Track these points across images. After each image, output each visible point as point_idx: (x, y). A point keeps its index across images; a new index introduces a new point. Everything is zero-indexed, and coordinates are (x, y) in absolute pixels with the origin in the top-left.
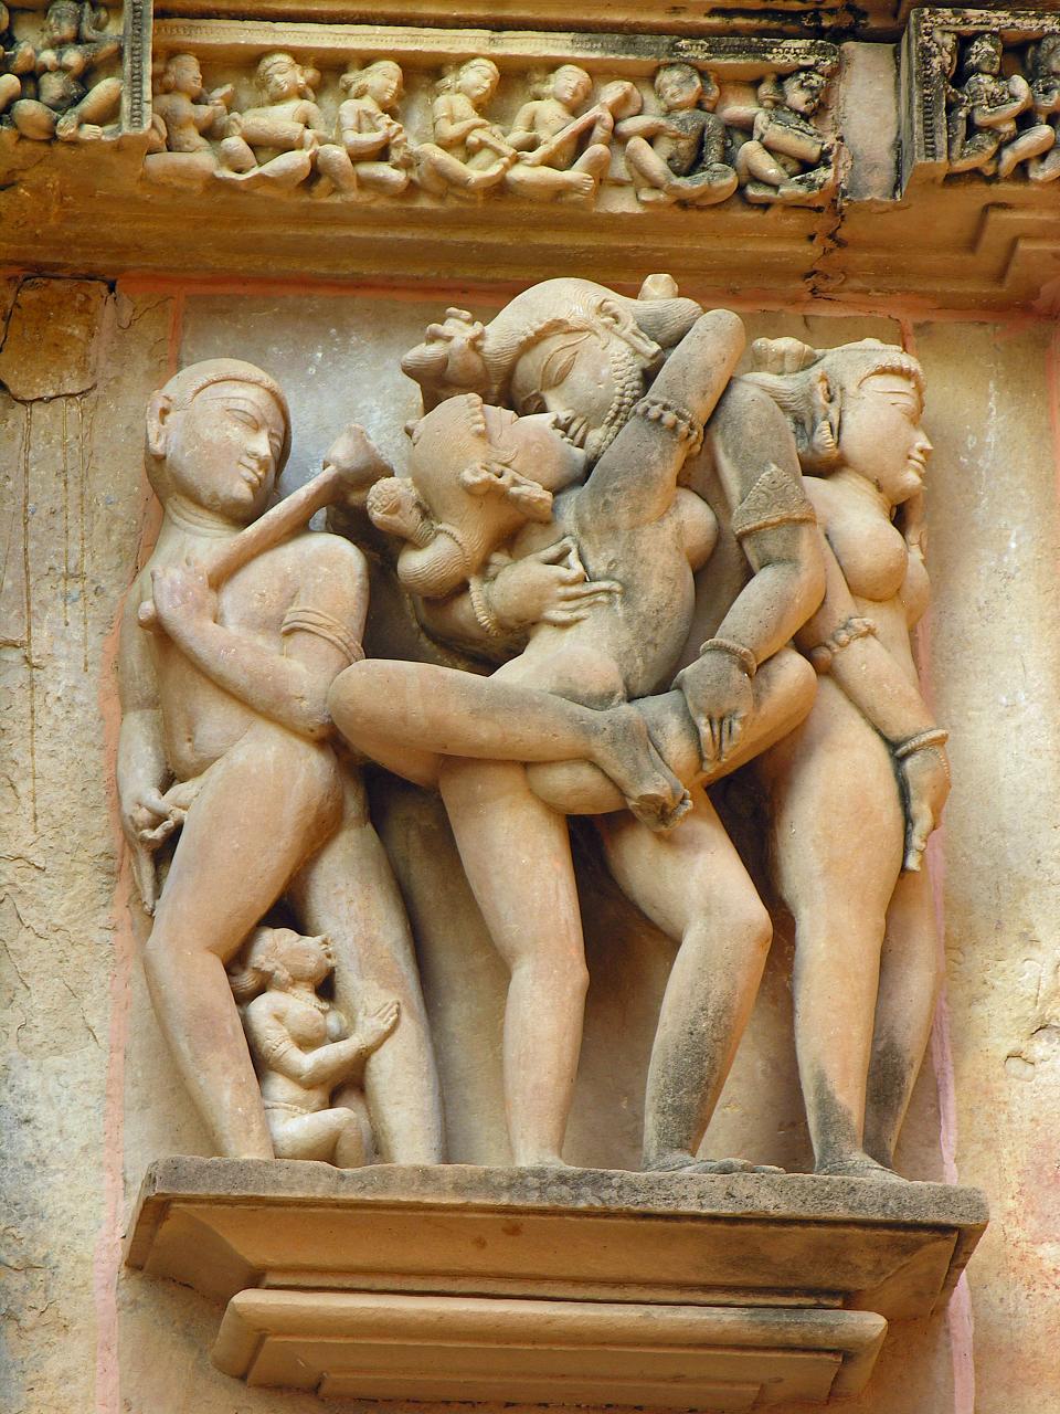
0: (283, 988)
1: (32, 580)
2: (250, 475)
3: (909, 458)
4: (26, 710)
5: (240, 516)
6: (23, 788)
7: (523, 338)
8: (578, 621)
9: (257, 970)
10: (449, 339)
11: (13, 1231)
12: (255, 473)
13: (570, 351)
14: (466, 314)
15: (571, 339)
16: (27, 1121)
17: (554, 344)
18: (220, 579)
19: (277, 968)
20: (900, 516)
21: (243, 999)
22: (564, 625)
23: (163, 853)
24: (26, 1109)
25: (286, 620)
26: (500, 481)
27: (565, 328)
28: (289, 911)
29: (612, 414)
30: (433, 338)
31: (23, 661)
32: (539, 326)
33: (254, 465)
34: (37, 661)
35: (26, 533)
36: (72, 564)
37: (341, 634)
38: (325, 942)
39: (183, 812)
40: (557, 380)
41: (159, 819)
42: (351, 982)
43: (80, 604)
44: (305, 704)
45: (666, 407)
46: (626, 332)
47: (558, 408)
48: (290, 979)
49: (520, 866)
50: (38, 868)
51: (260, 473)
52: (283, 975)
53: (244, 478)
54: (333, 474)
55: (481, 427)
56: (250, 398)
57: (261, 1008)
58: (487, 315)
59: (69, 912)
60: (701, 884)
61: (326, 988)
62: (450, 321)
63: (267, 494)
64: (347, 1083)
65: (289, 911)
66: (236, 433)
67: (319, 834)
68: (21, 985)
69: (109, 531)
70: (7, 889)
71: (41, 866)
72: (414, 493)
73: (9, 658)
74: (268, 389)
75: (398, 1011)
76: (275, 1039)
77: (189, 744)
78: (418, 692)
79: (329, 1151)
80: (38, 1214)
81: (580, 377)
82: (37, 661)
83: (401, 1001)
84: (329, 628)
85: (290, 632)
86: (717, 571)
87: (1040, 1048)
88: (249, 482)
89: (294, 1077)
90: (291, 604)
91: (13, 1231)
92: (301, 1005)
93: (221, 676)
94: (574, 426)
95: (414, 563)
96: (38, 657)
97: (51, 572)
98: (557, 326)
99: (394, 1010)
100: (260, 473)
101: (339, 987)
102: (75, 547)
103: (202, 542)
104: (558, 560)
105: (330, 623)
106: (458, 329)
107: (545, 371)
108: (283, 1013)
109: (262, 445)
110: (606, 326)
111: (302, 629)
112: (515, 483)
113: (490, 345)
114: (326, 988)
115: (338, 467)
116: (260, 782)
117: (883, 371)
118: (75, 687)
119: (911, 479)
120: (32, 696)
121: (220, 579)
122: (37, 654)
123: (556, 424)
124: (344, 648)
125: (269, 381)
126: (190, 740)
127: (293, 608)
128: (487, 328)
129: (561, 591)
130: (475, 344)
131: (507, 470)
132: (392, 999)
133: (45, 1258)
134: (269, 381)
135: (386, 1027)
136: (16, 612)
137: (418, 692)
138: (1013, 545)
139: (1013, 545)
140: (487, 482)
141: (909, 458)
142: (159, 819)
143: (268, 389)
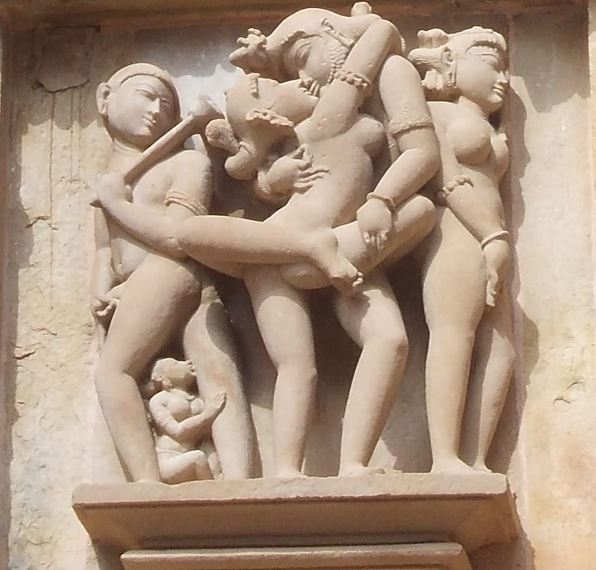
0: (168, 389)
1: (53, 184)
2: (150, 123)
3: (494, 88)
4: (48, 251)
5: (142, 143)
6: (47, 292)
7: (283, 42)
8: (309, 187)
9: (154, 381)
10: (247, 46)
11: (34, 524)
12: (151, 121)
13: (308, 46)
14: (258, 31)
15: (308, 41)
16: (43, 467)
17: (299, 43)
18: (132, 178)
19: (163, 380)
20: (495, 118)
21: (146, 396)
22: (303, 191)
23: (106, 322)
24: (43, 461)
25: (167, 197)
26: (265, 118)
27: (304, 35)
28: (174, 348)
29: (330, 77)
30: (242, 45)
31: (48, 226)
32: (291, 35)
33: (151, 117)
34: (55, 226)
35: (51, 161)
36: (74, 174)
37: (192, 203)
38: (190, 364)
39: (117, 300)
40: (302, 61)
41: (105, 304)
42: (202, 384)
43: (77, 195)
44: (173, 240)
45: (349, 73)
46: (336, 35)
47: (304, 76)
48: (171, 385)
49: (282, 321)
50: (53, 334)
51: (154, 122)
52: (166, 383)
53: (146, 124)
54: (190, 120)
55: (255, 90)
56: (150, 84)
57: (155, 401)
58: (267, 28)
59: (67, 357)
60: (379, 323)
61: (192, 387)
62: (250, 35)
63: (158, 130)
64: (201, 438)
65: (174, 348)
66: (141, 100)
67: (185, 306)
68: (42, 396)
69: (93, 156)
70: (36, 347)
71: (55, 333)
72: (228, 126)
73: (41, 225)
74: (159, 78)
75: (225, 398)
76: (163, 417)
77: (120, 265)
78: (236, 230)
79: (191, 474)
80: (48, 515)
81: (313, 60)
82: (55, 226)
83: (227, 393)
84: (186, 200)
85: (168, 204)
86: (380, 157)
87: (572, 394)
88: (149, 126)
89: (172, 436)
90: (170, 189)
91: (34, 524)
92: (177, 398)
93: (130, 229)
94: (313, 85)
95: (231, 163)
96: (55, 224)
97: (64, 179)
98: (299, 35)
99: (222, 397)
100: (154, 122)
101: (200, 388)
102: (76, 165)
103: (132, 158)
104: (300, 156)
105: (186, 197)
106: (253, 38)
107: (297, 58)
108: (166, 404)
109: (155, 107)
110: (328, 32)
111: (173, 202)
112: (273, 118)
113: (269, 47)
114: (192, 387)
115: (193, 115)
116: (156, 280)
117: (478, 44)
118: (73, 238)
119: (496, 98)
120: (52, 245)
121: (132, 178)
122: (55, 222)
123: (302, 85)
124: (194, 209)
125: (164, 74)
126: (120, 263)
127: (171, 190)
128: (268, 38)
129: (300, 172)
130: (260, 47)
131: (268, 111)
132: (222, 391)
133: (51, 538)
134: (164, 74)
135: (219, 407)
136: (44, 201)
137: (236, 230)
138: (564, 128)
139: (564, 128)
140: (257, 119)
141: (494, 88)
142: (105, 304)
143: (159, 78)
